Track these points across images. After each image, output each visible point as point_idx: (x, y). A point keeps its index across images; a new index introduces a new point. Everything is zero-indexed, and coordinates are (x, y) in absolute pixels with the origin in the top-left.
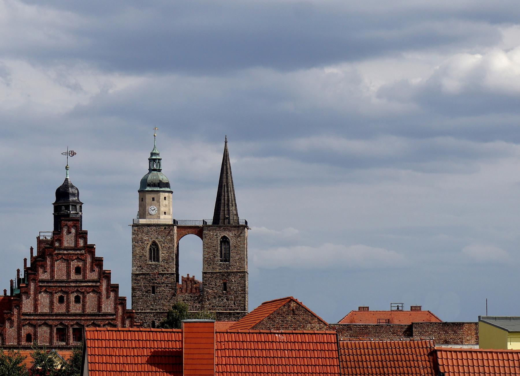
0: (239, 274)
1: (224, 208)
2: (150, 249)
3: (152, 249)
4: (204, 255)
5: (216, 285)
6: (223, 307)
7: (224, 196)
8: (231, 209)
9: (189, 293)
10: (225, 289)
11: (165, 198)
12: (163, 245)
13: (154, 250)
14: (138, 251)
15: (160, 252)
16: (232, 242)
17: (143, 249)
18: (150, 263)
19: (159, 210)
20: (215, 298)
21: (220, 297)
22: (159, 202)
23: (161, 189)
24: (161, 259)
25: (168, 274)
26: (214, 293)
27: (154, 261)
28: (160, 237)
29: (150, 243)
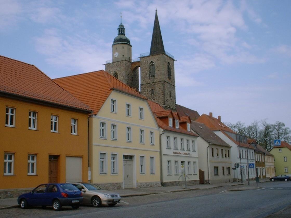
5: (148, 92)
12: (120, 73)
28: (118, 68)
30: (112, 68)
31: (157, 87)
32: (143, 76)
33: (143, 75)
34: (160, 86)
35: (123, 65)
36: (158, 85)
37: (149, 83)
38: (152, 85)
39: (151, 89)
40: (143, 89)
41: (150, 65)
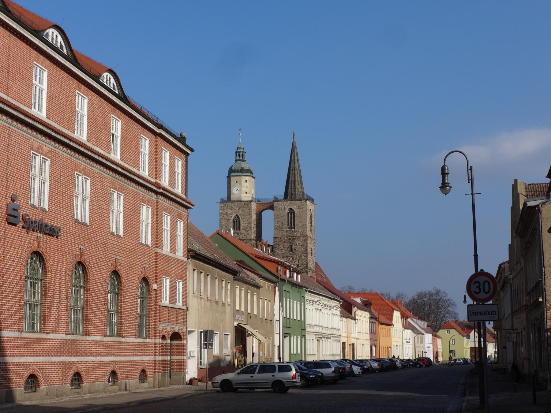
2: (234, 221)
10: (292, 251)
15: (241, 223)
16: (297, 212)
19: (241, 190)
21: (287, 257)
22: (240, 184)
24: (241, 228)
28: (241, 211)
29: (234, 215)
30: (231, 209)
35: (247, 207)
41: (288, 213)
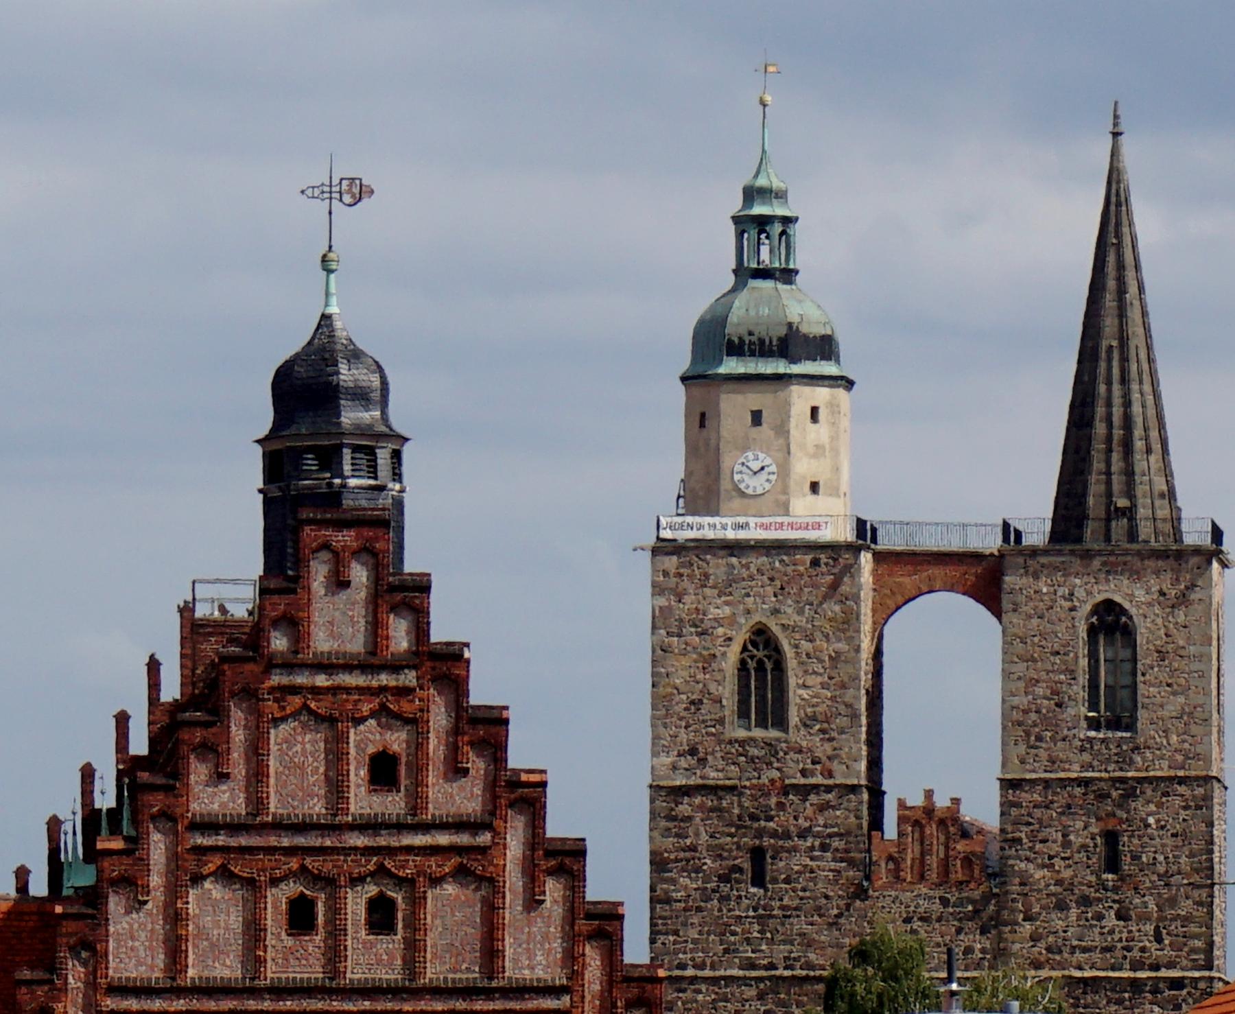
0: (1181, 789)
1: (1108, 463)
2: (743, 667)
3: (752, 665)
4: (1007, 694)
5: (1066, 844)
6: (1106, 950)
7: (1109, 404)
8: (1140, 463)
9: (938, 885)
10: (1112, 863)
11: (814, 411)
13: (760, 667)
14: (681, 670)
15: (792, 681)
16: (1148, 628)
17: (708, 661)
18: (742, 734)
19: (784, 471)
20: (1062, 906)
21: (1085, 901)
22: (782, 430)
23: (796, 369)
24: (794, 718)
25: (829, 789)
26: (1059, 882)
27: (762, 723)
28: (789, 608)
29: (741, 637)
30: (725, 589)
31: (1151, 820)
32: (1026, 712)
33: (1022, 701)
34: (1183, 814)
36: (1160, 805)
37: (1085, 783)
38: (1109, 796)
39: (1094, 829)
40: (1029, 815)
